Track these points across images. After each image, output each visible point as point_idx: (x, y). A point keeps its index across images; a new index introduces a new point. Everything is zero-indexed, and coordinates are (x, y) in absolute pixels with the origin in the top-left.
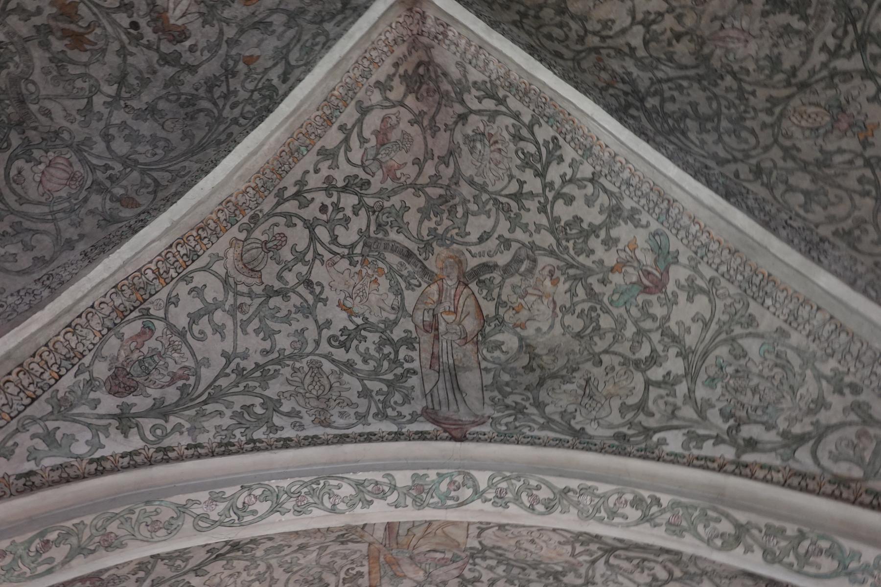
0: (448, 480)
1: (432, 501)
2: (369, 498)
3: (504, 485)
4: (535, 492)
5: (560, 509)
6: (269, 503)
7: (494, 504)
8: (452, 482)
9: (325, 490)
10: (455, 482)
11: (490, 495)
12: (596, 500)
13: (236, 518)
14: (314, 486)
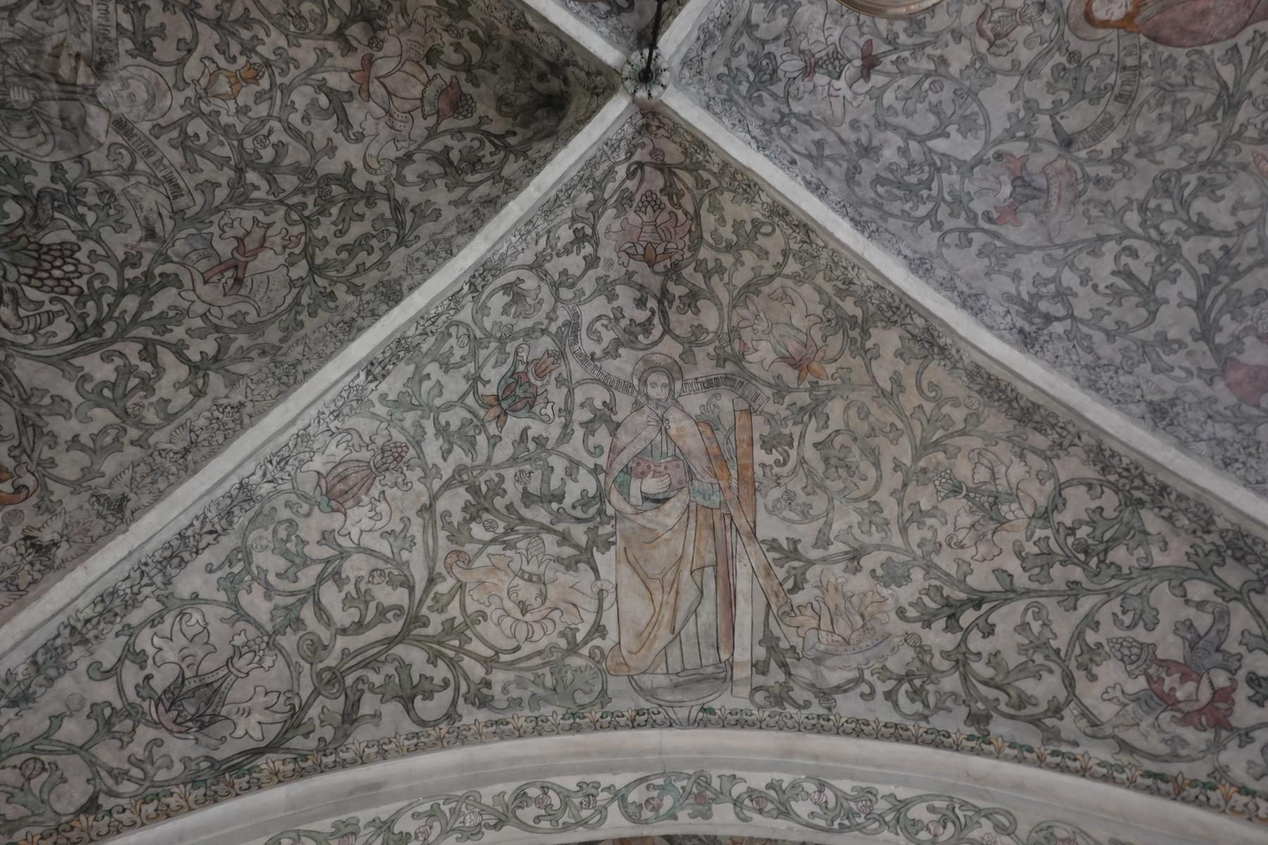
0: (662, 811)
1: (684, 783)
2: (772, 793)
3: (585, 813)
4: (542, 812)
7: (596, 785)
8: (656, 809)
9: (832, 814)
10: (653, 809)
11: (603, 796)
12: (457, 824)
14: (846, 822)
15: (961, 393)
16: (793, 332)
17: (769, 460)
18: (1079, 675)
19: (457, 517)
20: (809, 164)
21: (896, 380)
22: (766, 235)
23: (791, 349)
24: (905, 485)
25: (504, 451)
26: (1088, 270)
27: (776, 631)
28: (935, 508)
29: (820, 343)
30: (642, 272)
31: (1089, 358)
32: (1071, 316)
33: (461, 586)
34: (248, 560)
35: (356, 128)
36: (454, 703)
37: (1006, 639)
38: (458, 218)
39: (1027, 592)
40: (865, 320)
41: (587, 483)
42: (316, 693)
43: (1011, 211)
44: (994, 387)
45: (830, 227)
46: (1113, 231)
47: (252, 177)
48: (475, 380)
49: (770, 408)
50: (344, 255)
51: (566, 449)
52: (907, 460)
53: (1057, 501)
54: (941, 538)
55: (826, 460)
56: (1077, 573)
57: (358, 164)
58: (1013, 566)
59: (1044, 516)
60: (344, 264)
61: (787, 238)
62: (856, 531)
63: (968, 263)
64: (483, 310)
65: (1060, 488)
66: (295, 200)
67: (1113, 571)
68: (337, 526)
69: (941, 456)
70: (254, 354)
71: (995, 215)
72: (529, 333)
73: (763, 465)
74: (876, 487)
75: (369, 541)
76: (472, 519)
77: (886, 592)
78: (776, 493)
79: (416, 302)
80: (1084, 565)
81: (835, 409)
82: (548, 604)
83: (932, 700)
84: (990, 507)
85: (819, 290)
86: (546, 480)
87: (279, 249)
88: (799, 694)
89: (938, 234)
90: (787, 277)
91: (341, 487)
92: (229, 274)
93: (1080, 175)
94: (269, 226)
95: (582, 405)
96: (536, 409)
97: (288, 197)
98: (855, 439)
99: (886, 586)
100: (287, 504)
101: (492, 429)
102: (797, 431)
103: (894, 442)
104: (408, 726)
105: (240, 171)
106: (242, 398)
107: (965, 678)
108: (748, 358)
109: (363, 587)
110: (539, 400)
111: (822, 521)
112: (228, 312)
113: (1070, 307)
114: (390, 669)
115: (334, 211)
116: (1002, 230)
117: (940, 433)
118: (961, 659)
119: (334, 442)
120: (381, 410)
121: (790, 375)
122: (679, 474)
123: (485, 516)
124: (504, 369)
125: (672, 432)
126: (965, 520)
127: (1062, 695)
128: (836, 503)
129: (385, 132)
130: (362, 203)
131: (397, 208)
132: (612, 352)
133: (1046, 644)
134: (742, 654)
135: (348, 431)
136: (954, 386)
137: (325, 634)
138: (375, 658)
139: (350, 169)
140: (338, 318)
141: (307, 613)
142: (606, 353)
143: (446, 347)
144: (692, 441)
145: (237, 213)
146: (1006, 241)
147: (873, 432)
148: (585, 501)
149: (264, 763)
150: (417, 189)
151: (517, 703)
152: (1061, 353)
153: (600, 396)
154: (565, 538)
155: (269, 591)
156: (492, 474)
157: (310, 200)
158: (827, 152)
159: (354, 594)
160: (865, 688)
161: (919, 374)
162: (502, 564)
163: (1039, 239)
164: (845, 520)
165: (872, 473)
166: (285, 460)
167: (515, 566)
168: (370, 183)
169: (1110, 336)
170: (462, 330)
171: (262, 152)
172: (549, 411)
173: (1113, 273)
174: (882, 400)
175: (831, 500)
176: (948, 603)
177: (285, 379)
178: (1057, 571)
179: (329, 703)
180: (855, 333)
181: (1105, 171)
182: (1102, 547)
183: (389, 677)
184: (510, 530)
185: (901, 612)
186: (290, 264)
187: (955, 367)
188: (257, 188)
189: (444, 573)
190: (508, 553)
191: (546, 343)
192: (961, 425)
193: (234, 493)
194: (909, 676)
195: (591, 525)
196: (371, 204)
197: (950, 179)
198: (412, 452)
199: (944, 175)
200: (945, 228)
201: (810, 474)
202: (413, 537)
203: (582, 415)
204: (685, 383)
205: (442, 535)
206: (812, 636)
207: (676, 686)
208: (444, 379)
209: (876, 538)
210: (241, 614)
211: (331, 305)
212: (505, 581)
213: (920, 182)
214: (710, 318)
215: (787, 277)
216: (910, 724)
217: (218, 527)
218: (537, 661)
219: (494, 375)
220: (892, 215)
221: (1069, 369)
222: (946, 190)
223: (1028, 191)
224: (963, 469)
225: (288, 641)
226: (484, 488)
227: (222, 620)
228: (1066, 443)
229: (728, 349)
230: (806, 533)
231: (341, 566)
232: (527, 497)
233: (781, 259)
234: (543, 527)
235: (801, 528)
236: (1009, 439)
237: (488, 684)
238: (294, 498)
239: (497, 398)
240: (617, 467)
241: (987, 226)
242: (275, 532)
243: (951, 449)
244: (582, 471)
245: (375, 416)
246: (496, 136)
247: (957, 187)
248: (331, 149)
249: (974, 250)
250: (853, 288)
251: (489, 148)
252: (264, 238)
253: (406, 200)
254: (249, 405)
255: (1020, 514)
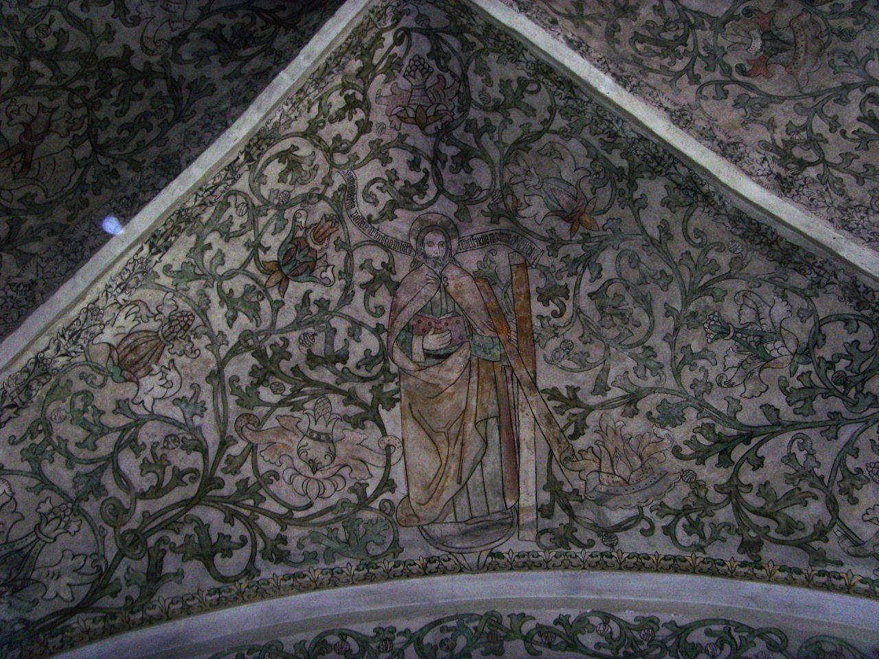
0: (456, 651)
1: (476, 624)
2: (560, 628)
5: (307, 645)
6: (689, 640)
7: (393, 630)
9: (617, 644)
10: (448, 649)
13: (733, 633)
14: (631, 650)
15: (726, 239)
16: (564, 186)
17: (546, 311)
18: (841, 499)
19: (245, 381)
20: (569, 24)
21: (664, 228)
22: (532, 93)
23: (562, 203)
24: (676, 329)
25: (287, 317)
26: (835, 118)
27: (559, 476)
28: (705, 349)
29: (589, 196)
30: (416, 137)
31: (840, 201)
32: (823, 161)
33: (252, 448)
34: (48, 431)
35: (133, 13)
36: (252, 559)
37: (774, 470)
38: (232, 92)
39: (793, 425)
40: (631, 171)
41: (370, 342)
42: (120, 555)
43: (762, 65)
44: (757, 231)
45: (594, 83)
46: (857, 80)
47: (35, 64)
48: (256, 247)
49: (545, 261)
50: (125, 134)
51: (345, 310)
52: (678, 306)
53: (817, 338)
54: (712, 377)
55: (601, 309)
56: (837, 404)
57: (135, 47)
58: (778, 400)
59: (805, 352)
60: (126, 141)
61: (553, 95)
62: (632, 376)
63: (726, 115)
64: (260, 178)
65: (819, 324)
66: (77, 84)
67: (869, 400)
68: (130, 395)
69: (709, 300)
70: (43, 233)
71: (748, 68)
72: (306, 199)
73: (541, 317)
74: (649, 334)
75: (160, 408)
76: (260, 383)
77: (662, 433)
78: (554, 344)
79: (195, 173)
80: (843, 397)
81: (607, 259)
82: (337, 461)
83: (707, 532)
84: (755, 345)
85: (586, 144)
86: (329, 342)
87: (63, 131)
88: (583, 534)
89: (696, 87)
90: (555, 132)
91: (132, 357)
92: (17, 158)
93: (824, 28)
94: (55, 110)
95: (362, 267)
96: (317, 273)
97: (72, 81)
98: (628, 288)
99: (663, 427)
100: (82, 377)
101: (275, 295)
102: (572, 281)
103: (665, 288)
104: (210, 582)
105: (24, 60)
106: (32, 276)
107: (737, 509)
108: (522, 213)
109: (159, 452)
110: (319, 264)
111: (599, 368)
112: (19, 194)
113: (821, 153)
114: (189, 530)
115: (115, 92)
116: (755, 82)
117: (707, 278)
118: (733, 492)
119: (122, 315)
120: (166, 281)
121: (563, 229)
122: (460, 330)
123: (273, 379)
124: (283, 236)
125: (451, 288)
126: (734, 360)
127: (827, 519)
128: (613, 350)
129: (160, 15)
130: (141, 83)
131: (174, 86)
132: (388, 214)
133: (811, 472)
134: (527, 500)
135: (135, 303)
136: (717, 231)
137: (126, 500)
138: (174, 520)
139: (128, 52)
140: (121, 194)
141: (108, 480)
142: (383, 215)
143: (226, 216)
144: (471, 297)
145: (21, 100)
146: (760, 93)
147: (643, 281)
148: (368, 360)
149: (78, 622)
150: (191, 66)
151: (313, 557)
152: (815, 196)
153: (379, 257)
154: (350, 398)
155: (70, 461)
156: (276, 338)
157: (92, 84)
158: (587, 12)
159: (151, 460)
160: (645, 525)
161: (685, 221)
162: (290, 426)
163: (790, 90)
164: (622, 366)
165: (645, 320)
166: (76, 335)
167: (303, 426)
168: (147, 64)
169: (860, 179)
170: (241, 199)
171: (46, 41)
172: (329, 274)
173: (859, 119)
174: (651, 248)
175: (607, 347)
176: (720, 439)
177: (72, 256)
178: (819, 404)
179: (133, 564)
180: (622, 185)
181: (848, 23)
182: (859, 378)
183: (188, 536)
184: (297, 392)
185: (676, 451)
186: (74, 146)
187: (718, 214)
188: (41, 75)
189: (236, 435)
190: (296, 414)
191: (323, 208)
192: (726, 269)
193: (31, 367)
194: (686, 511)
195: (376, 383)
196: (149, 83)
197: (704, 35)
198: (198, 321)
199: (698, 31)
200: (703, 81)
201: (586, 323)
202: (204, 403)
203: (362, 277)
204: (461, 241)
205: (232, 399)
206: (593, 480)
207: (464, 534)
208: (226, 248)
209: (651, 382)
210: (46, 483)
211: (115, 182)
212: (293, 441)
213: (676, 38)
214: (482, 176)
215: (555, 132)
216: (687, 555)
217: (17, 401)
218: (330, 516)
219: (273, 241)
220: (653, 70)
221: (823, 211)
222: (701, 45)
223: (777, 45)
224: (730, 312)
225: (92, 506)
226: (269, 352)
227: (29, 489)
228: (824, 281)
229: (502, 206)
230: (584, 380)
231: (136, 433)
232: (313, 360)
233: (547, 116)
234: (329, 388)
235: (580, 376)
236: (771, 281)
237: (284, 541)
238: (88, 370)
239: (278, 264)
240: (399, 326)
241: (740, 78)
242: (72, 404)
243: (718, 293)
244: (365, 331)
245: (161, 287)
246: (266, 11)
247: (711, 42)
248: (110, 34)
249: (730, 101)
250: (618, 141)
251: (260, 22)
252: (49, 123)
253: (182, 78)
254: (41, 282)
255: (783, 351)
